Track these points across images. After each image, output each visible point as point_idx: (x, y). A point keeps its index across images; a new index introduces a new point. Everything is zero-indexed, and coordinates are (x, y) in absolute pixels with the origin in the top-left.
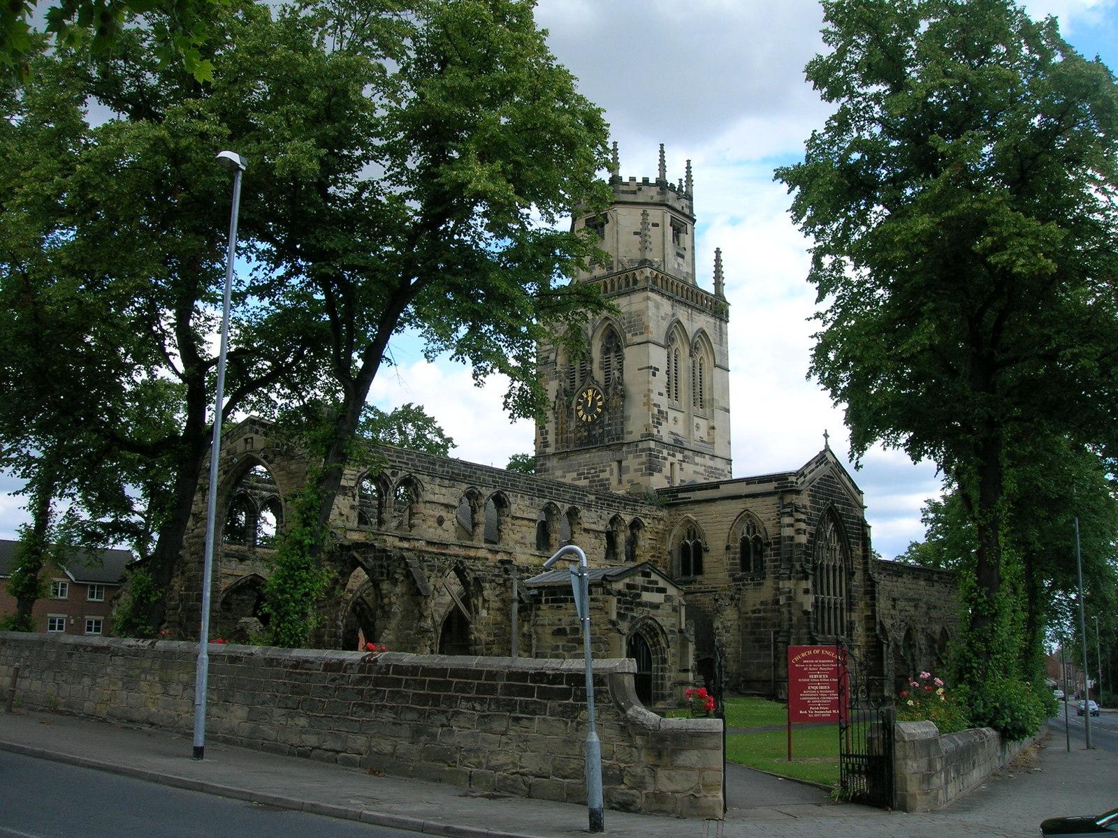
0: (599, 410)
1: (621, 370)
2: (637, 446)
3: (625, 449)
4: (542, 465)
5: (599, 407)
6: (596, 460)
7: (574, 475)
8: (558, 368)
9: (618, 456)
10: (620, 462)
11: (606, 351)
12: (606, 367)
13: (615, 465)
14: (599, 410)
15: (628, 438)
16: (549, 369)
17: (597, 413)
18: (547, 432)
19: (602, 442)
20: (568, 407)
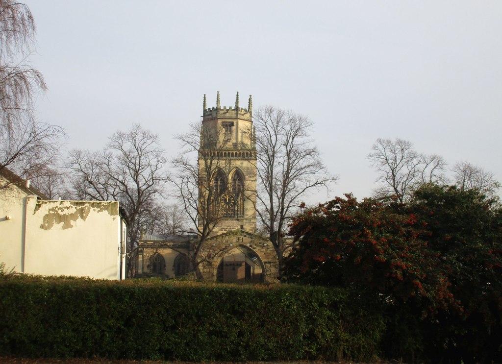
3: (244, 221)
17: (231, 205)
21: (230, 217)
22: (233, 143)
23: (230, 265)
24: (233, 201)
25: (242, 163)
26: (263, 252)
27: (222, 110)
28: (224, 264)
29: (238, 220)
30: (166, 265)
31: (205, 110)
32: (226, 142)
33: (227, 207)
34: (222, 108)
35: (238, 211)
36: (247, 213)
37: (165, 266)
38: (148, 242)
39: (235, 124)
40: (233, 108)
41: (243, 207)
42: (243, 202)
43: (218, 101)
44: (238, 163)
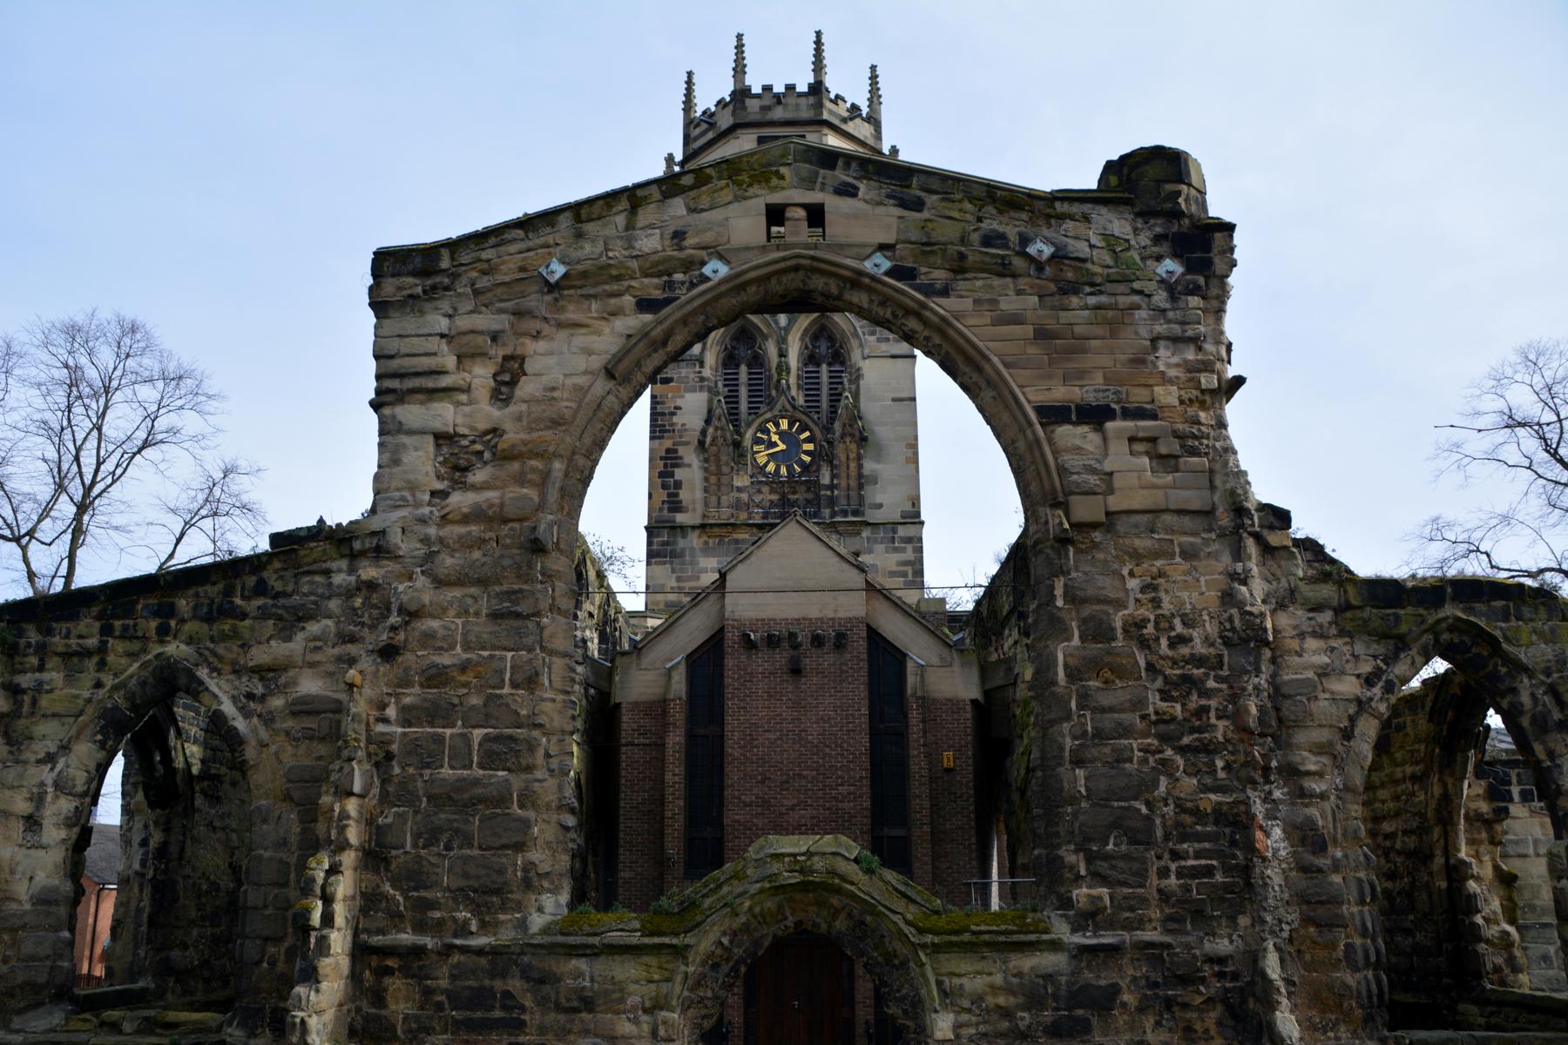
0: (807, 459)
1: (856, 396)
2: (895, 531)
5: (807, 453)
8: (707, 372)
11: (811, 359)
12: (810, 385)
14: (807, 459)
15: (873, 516)
18: (678, 485)
20: (737, 445)
23: (772, 641)
26: (1016, 319)
27: (757, 96)
28: (731, 636)
31: (689, 123)
33: (783, 471)
34: (756, 90)
36: (879, 499)
40: (802, 87)
43: (739, 69)
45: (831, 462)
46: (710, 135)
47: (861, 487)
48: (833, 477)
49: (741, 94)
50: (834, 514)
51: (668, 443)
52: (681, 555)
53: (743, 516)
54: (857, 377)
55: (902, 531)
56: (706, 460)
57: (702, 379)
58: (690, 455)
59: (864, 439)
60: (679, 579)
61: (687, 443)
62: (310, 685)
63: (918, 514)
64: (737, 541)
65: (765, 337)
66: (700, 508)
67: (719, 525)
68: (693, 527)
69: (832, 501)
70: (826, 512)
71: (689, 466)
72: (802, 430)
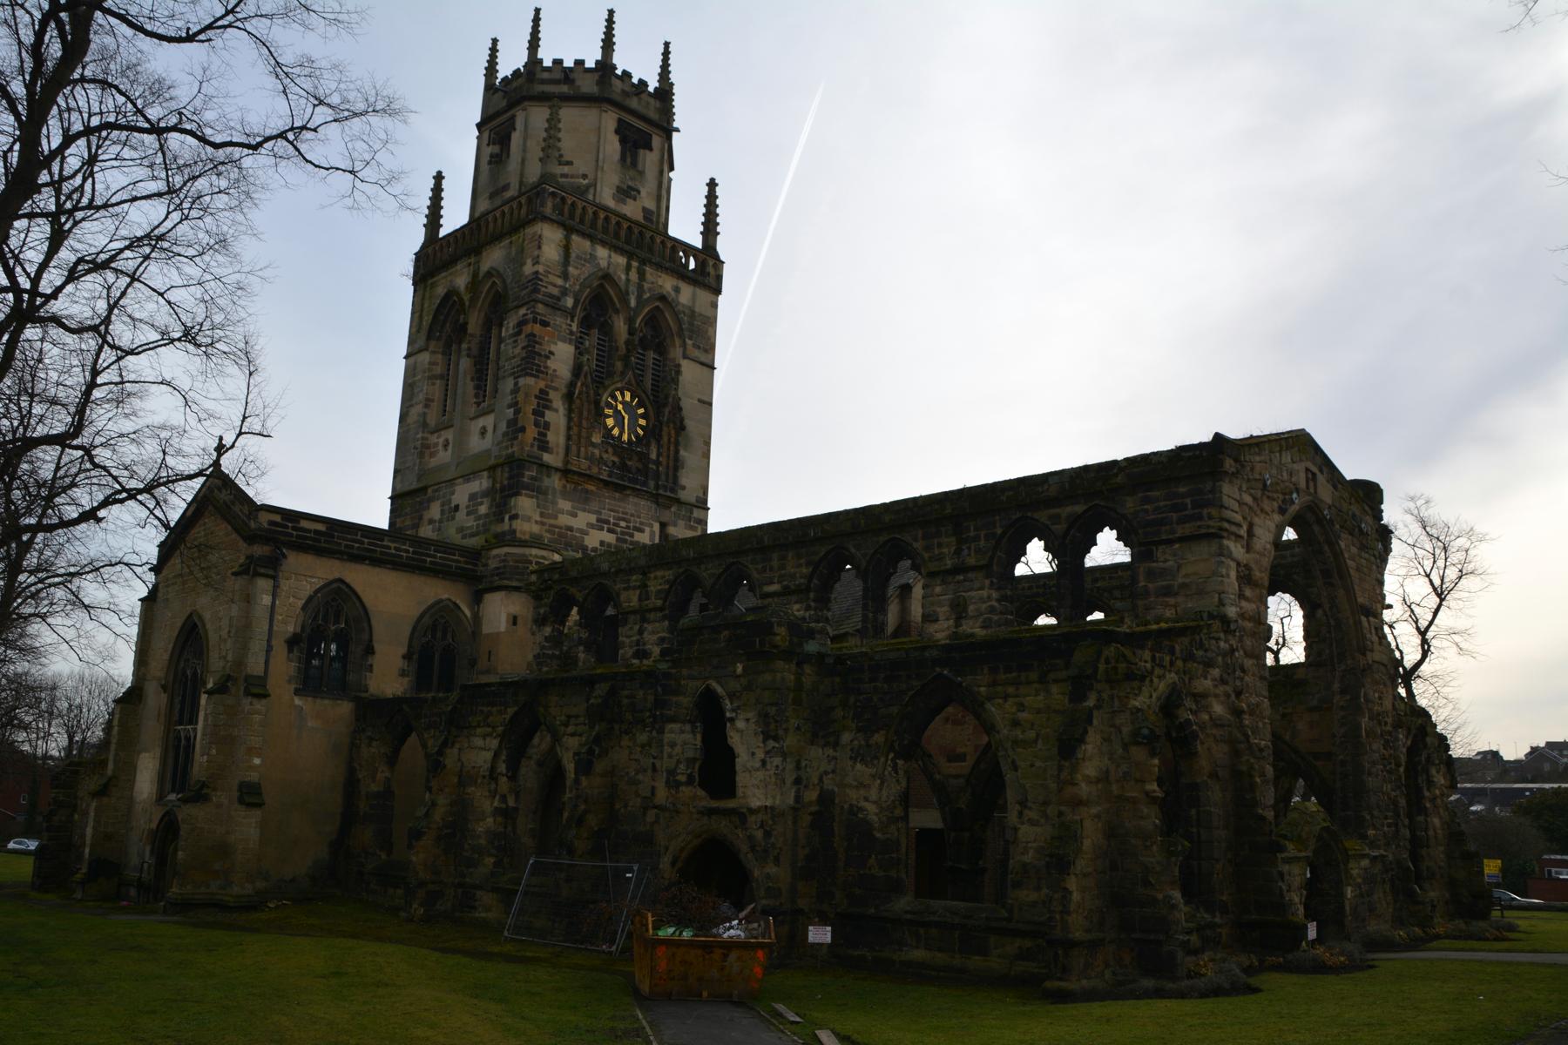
0: (641, 432)
4: (533, 478)
5: (642, 427)
6: (630, 508)
7: (593, 518)
9: (667, 516)
10: (663, 526)
13: (657, 527)
14: (641, 432)
15: (684, 495)
16: (558, 320)
18: (547, 426)
19: (645, 484)
20: (597, 403)
21: (630, 480)
22: (644, 209)
24: (642, 422)
25: (677, 290)
29: (655, 498)
30: (377, 646)
32: (626, 192)
35: (658, 463)
37: (370, 650)
38: (304, 524)
39: (656, 141)
40: (651, 89)
41: (677, 452)
42: (678, 435)
44: (667, 283)
45: (658, 442)
46: (565, 89)
47: (676, 469)
48: (659, 455)
49: (605, 65)
50: (657, 487)
51: (542, 384)
52: (545, 493)
53: (595, 470)
54: (678, 372)
55: (696, 513)
56: (570, 411)
57: (571, 333)
58: (558, 402)
59: (683, 428)
60: (542, 515)
61: (556, 389)
62: (1218, 709)
63: (705, 501)
64: (587, 491)
65: (617, 312)
66: (562, 451)
67: (580, 474)
68: (557, 470)
69: (657, 476)
70: (652, 484)
71: (556, 411)
72: (640, 405)
